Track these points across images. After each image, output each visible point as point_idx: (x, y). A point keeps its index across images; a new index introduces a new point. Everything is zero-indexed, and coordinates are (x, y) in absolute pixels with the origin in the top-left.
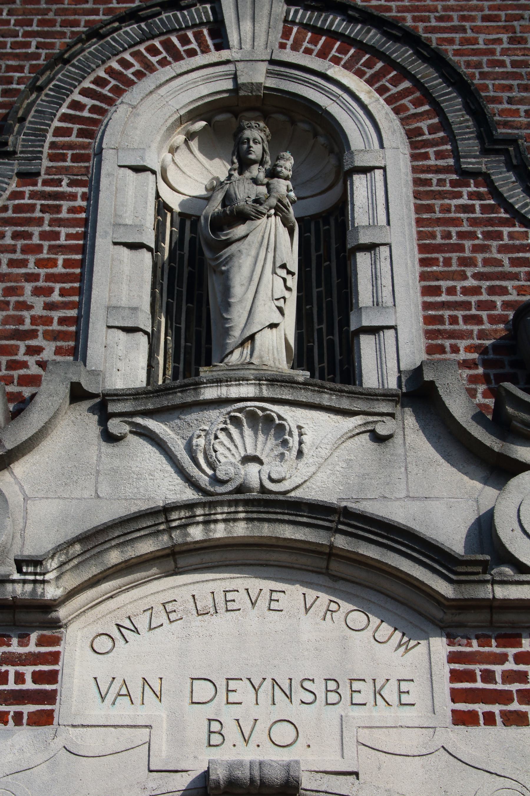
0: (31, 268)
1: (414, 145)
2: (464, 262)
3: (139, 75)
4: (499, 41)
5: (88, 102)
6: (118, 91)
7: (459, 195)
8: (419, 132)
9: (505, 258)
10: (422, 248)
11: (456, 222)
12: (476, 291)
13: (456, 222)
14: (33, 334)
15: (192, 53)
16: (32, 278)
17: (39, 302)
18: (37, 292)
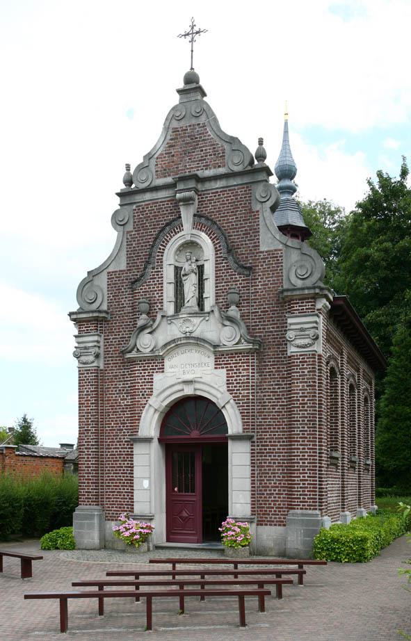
0: (156, 289)
1: (216, 251)
2: (223, 279)
3: (162, 256)
4: (233, 219)
5: (162, 247)
6: (166, 244)
7: (222, 263)
8: (216, 248)
9: (229, 278)
10: (216, 277)
11: (222, 270)
12: (223, 286)
13: (222, 270)
14: (156, 303)
15: (178, 232)
16: (156, 291)
17: (157, 296)
18: (158, 293)
